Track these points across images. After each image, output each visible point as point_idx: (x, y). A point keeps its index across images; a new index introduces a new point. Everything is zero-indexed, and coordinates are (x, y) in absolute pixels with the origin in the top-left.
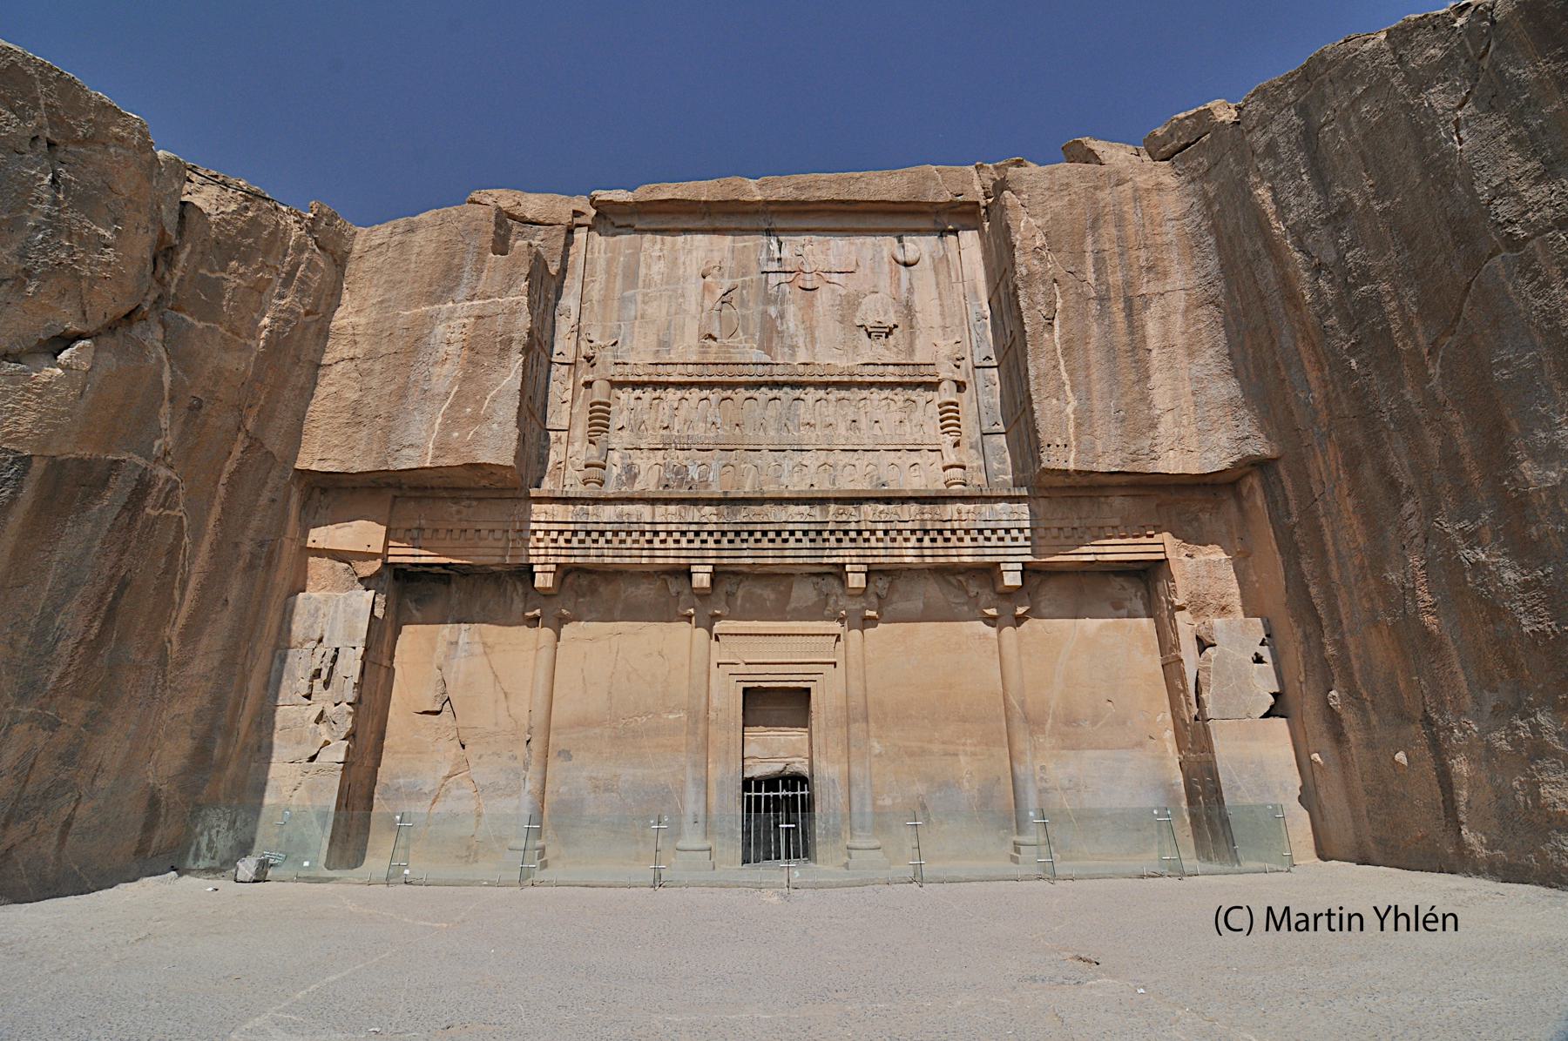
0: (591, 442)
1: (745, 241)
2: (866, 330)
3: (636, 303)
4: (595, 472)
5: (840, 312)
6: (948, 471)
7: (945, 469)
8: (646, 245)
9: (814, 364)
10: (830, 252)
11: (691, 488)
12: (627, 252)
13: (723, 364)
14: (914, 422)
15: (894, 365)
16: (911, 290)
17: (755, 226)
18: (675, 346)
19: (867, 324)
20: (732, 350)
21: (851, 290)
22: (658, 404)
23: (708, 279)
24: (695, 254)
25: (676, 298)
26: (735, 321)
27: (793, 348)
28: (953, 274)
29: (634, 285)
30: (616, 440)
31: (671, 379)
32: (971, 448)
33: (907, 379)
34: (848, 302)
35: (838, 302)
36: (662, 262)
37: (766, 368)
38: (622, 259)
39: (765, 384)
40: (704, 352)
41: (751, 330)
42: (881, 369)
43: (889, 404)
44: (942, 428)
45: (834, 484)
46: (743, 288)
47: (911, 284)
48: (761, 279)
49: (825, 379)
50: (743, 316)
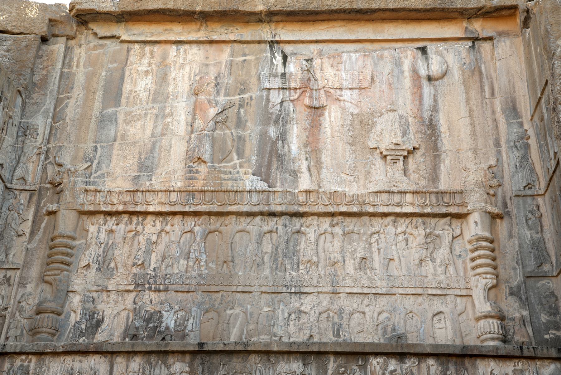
0: (47, 282)
1: (245, 55)
2: (381, 153)
3: (117, 124)
4: (47, 320)
5: (351, 133)
6: (482, 322)
7: (478, 319)
8: (131, 59)
9: (318, 192)
10: (342, 67)
11: (164, 339)
12: (111, 66)
13: (212, 191)
14: (438, 261)
15: (413, 193)
16: (435, 109)
17: (258, 39)
18: (159, 171)
19: (383, 147)
20: (223, 176)
21: (366, 106)
22: (134, 237)
23: (202, 97)
24: (187, 69)
25: (164, 117)
26: (229, 143)
27: (295, 174)
28: (487, 88)
29: (117, 103)
30: (79, 281)
31: (151, 209)
32: (511, 294)
33: (428, 210)
34: (361, 123)
35: (349, 122)
36: (150, 77)
37: (262, 196)
38: (104, 74)
39: (262, 214)
40: (191, 178)
41: (247, 153)
42: (397, 198)
43: (407, 240)
44: (473, 268)
45: (338, 335)
46: (241, 106)
47: (435, 100)
48: (261, 97)
49: (331, 209)
50: (239, 138)
